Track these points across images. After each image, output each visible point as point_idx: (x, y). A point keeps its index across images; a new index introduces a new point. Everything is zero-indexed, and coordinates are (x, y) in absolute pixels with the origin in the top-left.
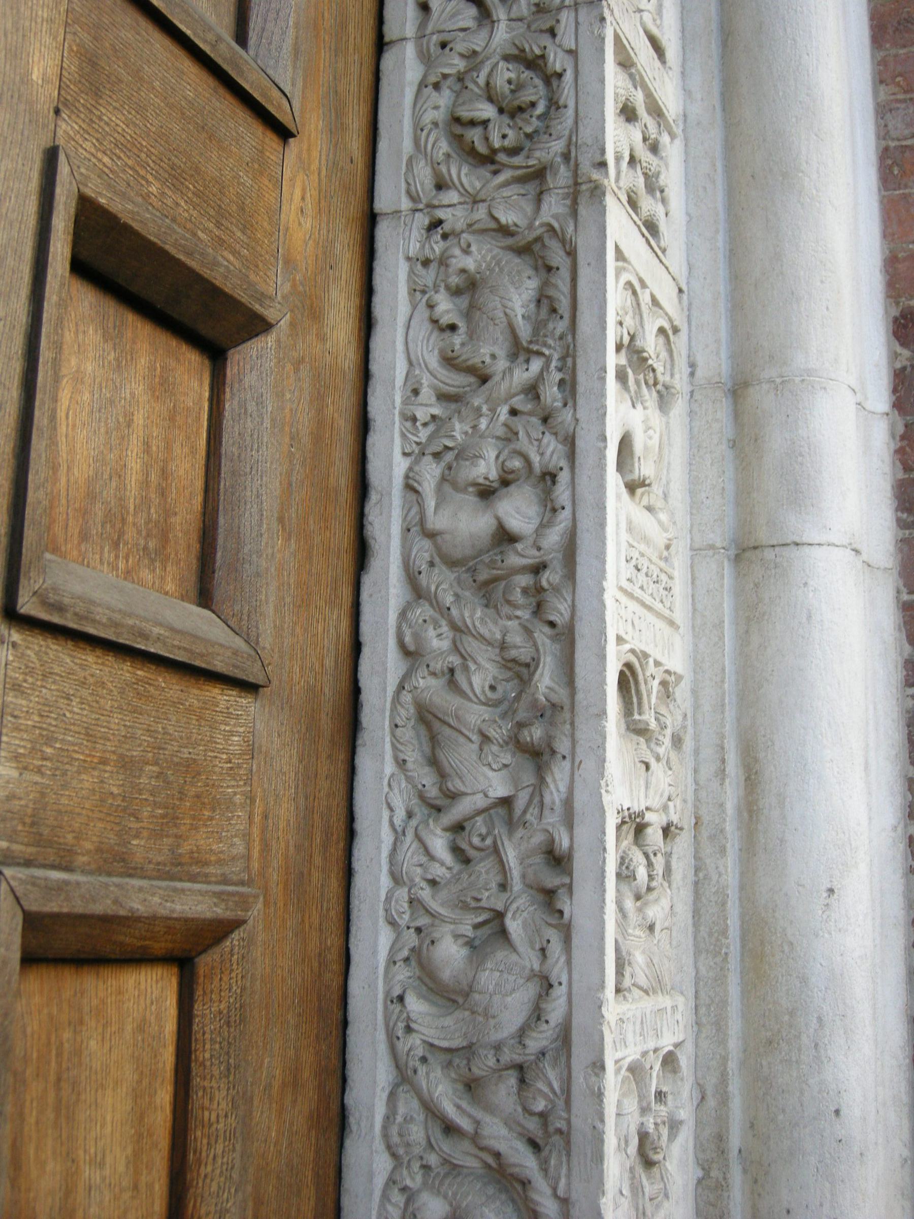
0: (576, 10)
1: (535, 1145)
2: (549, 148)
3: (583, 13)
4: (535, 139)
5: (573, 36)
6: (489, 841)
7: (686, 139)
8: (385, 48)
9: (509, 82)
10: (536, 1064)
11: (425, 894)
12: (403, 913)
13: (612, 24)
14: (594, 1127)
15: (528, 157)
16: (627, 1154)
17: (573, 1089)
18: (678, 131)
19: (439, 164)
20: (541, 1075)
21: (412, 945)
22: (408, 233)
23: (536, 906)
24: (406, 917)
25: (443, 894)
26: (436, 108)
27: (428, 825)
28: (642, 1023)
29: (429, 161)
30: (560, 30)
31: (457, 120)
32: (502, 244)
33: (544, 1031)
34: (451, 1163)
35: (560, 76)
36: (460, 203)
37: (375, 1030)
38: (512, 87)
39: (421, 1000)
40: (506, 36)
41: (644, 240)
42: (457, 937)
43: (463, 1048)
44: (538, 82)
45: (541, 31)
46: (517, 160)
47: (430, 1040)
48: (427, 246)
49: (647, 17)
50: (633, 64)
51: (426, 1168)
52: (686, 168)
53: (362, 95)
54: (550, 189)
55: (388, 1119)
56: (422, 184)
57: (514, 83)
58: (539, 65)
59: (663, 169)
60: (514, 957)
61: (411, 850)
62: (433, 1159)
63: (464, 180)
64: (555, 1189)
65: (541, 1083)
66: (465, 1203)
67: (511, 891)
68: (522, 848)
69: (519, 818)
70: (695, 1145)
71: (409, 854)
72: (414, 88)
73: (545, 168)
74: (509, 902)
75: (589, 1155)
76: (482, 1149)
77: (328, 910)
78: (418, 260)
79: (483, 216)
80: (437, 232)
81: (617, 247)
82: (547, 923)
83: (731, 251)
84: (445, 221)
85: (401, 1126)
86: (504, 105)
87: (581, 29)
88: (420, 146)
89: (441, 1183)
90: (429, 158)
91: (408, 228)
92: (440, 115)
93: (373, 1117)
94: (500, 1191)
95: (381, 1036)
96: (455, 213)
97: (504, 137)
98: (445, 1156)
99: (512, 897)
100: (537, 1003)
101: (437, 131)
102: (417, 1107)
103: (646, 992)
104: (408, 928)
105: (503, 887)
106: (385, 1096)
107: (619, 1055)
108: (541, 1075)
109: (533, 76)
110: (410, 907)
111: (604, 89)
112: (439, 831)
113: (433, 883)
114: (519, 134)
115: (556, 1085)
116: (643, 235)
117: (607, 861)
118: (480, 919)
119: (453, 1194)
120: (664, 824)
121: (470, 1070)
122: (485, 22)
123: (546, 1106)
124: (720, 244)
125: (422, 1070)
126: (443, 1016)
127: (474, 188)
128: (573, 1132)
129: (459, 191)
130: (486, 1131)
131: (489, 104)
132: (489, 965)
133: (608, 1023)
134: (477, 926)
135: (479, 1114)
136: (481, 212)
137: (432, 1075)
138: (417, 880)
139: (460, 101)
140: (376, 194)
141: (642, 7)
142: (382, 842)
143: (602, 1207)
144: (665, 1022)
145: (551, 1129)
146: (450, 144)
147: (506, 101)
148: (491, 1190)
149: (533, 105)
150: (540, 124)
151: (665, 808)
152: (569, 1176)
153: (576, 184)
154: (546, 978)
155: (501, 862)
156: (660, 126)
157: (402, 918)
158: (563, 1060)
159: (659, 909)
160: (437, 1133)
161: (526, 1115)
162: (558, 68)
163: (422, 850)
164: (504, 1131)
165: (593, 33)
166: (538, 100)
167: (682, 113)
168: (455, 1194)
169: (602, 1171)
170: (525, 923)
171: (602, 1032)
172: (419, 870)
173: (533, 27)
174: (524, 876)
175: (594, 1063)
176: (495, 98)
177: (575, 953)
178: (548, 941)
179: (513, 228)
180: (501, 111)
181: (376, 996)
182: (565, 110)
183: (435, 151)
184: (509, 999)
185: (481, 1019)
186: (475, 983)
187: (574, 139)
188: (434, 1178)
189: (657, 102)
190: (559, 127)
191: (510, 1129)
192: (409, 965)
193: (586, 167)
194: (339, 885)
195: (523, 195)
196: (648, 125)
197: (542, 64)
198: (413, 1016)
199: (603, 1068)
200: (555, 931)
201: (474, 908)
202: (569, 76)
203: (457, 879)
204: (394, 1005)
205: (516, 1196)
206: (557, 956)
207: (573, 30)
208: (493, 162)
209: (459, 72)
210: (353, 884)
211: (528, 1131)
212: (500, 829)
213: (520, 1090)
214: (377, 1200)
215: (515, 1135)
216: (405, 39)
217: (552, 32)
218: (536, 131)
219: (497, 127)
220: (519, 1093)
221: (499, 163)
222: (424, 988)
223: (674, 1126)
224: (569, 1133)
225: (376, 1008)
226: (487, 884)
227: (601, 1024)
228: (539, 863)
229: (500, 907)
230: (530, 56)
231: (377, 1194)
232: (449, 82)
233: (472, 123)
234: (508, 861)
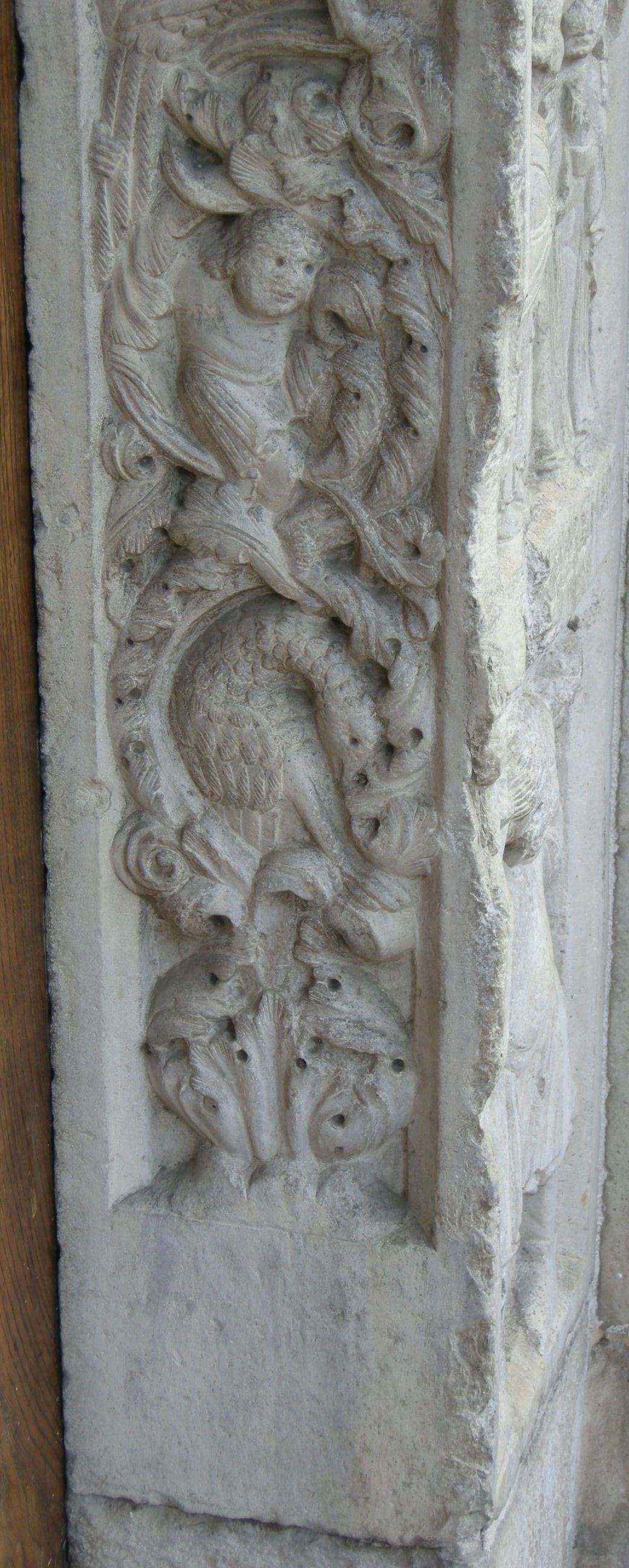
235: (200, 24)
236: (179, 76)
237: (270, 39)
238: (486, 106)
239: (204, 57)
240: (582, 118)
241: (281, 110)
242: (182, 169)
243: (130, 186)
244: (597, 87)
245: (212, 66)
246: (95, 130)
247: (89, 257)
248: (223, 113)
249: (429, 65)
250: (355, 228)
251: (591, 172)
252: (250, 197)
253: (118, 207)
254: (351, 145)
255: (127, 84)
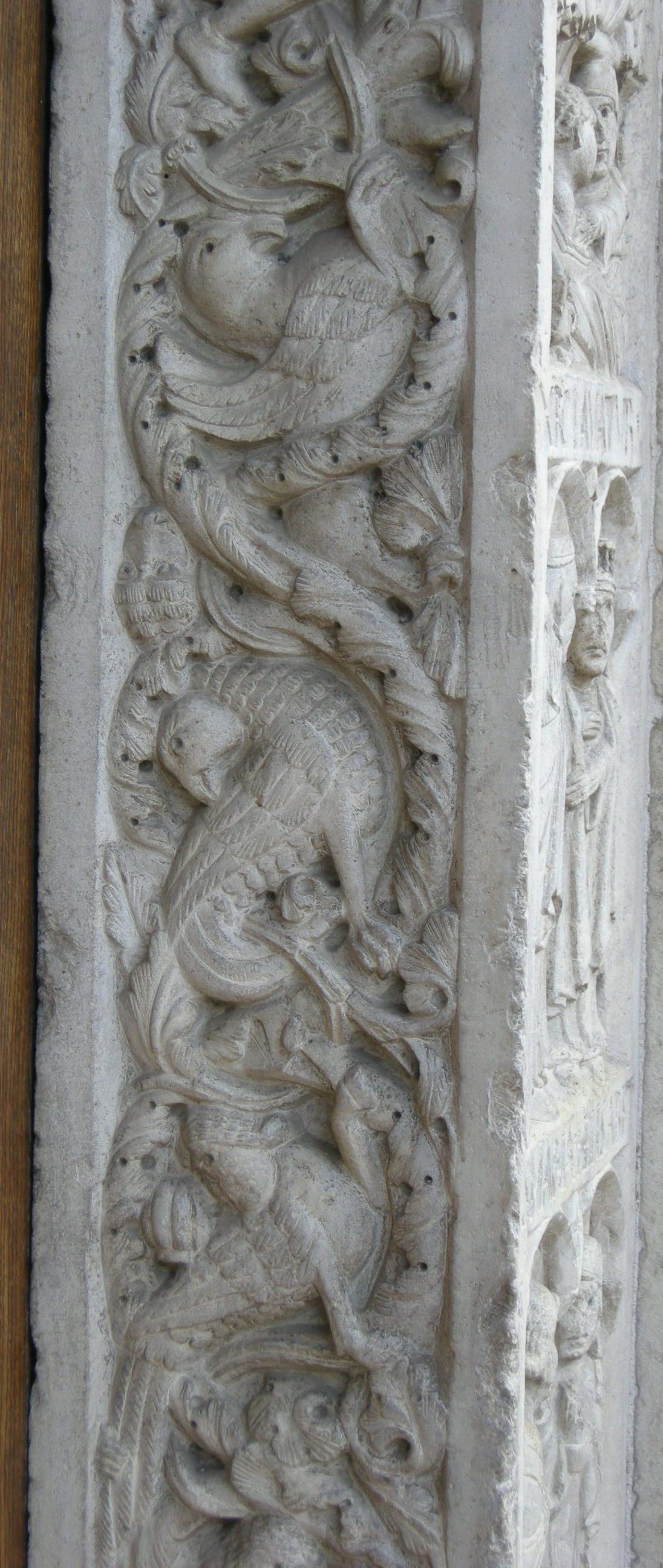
1: (401, 609)
6: (317, 59)
10: (407, 462)
11: (194, 159)
12: (153, 195)
14: (514, 570)
16: (558, 636)
17: (476, 504)
20: (416, 482)
21: (171, 254)
23: (406, 178)
24: (158, 203)
25: (230, 159)
27: (201, 29)
28: (584, 410)
33: (421, 403)
34: (244, 646)
37: (102, 411)
39: (189, 357)
42: (256, 236)
43: (268, 440)
47: (206, 428)
51: (198, 658)
55: (127, 574)
60: (366, 270)
61: (166, 77)
62: (211, 642)
64: (440, 684)
65: (417, 496)
66: (272, 717)
67: (359, 150)
68: (381, 68)
69: (376, 14)
70: (651, 661)
71: (163, 84)
74: (357, 168)
75: (504, 619)
76: (302, 619)
77: (14, 185)
82: (428, 206)
85: (152, 583)
89: (227, 685)
93: (99, 569)
94: (336, 693)
95: (113, 423)
98: (233, 634)
99: (362, 161)
100: (409, 354)
102: (182, 550)
103: (589, 355)
104: (162, 223)
105: (344, 144)
106: (120, 531)
107: (555, 452)
108: (416, 482)
110: (165, 185)
112: (221, 41)
113: (209, 139)
115: (443, 499)
117: (544, 89)
118: (300, 204)
119: (249, 702)
120: (618, 60)
121: (282, 477)
123: (423, 538)
125: (191, 481)
126: (228, 384)
128: (474, 582)
130: (311, 586)
132: (319, 286)
133: (541, 386)
134: (293, 218)
135: (298, 557)
137: (210, 490)
138: (179, 132)
142: (111, 63)
143: (527, 710)
144: (614, 422)
145: (434, 577)
148: (320, 693)
151: (618, 34)
152: (466, 659)
154: (427, 307)
155: (341, 96)
157: (150, 205)
158: (457, 452)
159: (610, 214)
160: (218, 597)
161: (387, 556)
163: (188, 77)
164: (345, 585)
168: (253, 702)
169: (529, 646)
170: (386, 209)
171: (530, 400)
172: (183, 115)
174: (383, 123)
175: (516, 457)
177: (484, 259)
178: (431, 240)
181: (102, 348)
184: (357, 346)
185: (302, 385)
186: (291, 321)
188: (213, 676)
191: (357, 581)
192: (164, 292)
194: (32, 143)
198: (173, 383)
199: (531, 465)
200: (445, 221)
201: (287, 184)
203: (254, 129)
204: (137, 366)
205: (365, 704)
206: (447, 265)
210: (54, 145)
211: (391, 583)
212: (338, 36)
213: (375, 510)
214: (109, 718)
215: (365, 591)
220: (373, 517)
222: (192, 336)
223: (624, 618)
224: (467, 585)
225: (103, 371)
226: (312, 137)
227: (530, 386)
228: (413, 98)
229: (338, 179)
231: (109, 707)
234: (355, 94)
235: (207, 1336)
236: (185, 1385)
237: (274, 1353)
238: (480, 1425)
239: (209, 1366)
240: (576, 1417)
241: (282, 1421)
242: (185, 1473)
243: (133, 1488)
244: (592, 1386)
245: (217, 1375)
246: (102, 1433)
247: (91, 1555)
248: (227, 1421)
249: (426, 1383)
250: (352, 1537)
251: (586, 1469)
252: (250, 1504)
253: (122, 1508)
254: (349, 1456)
255: (135, 1390)
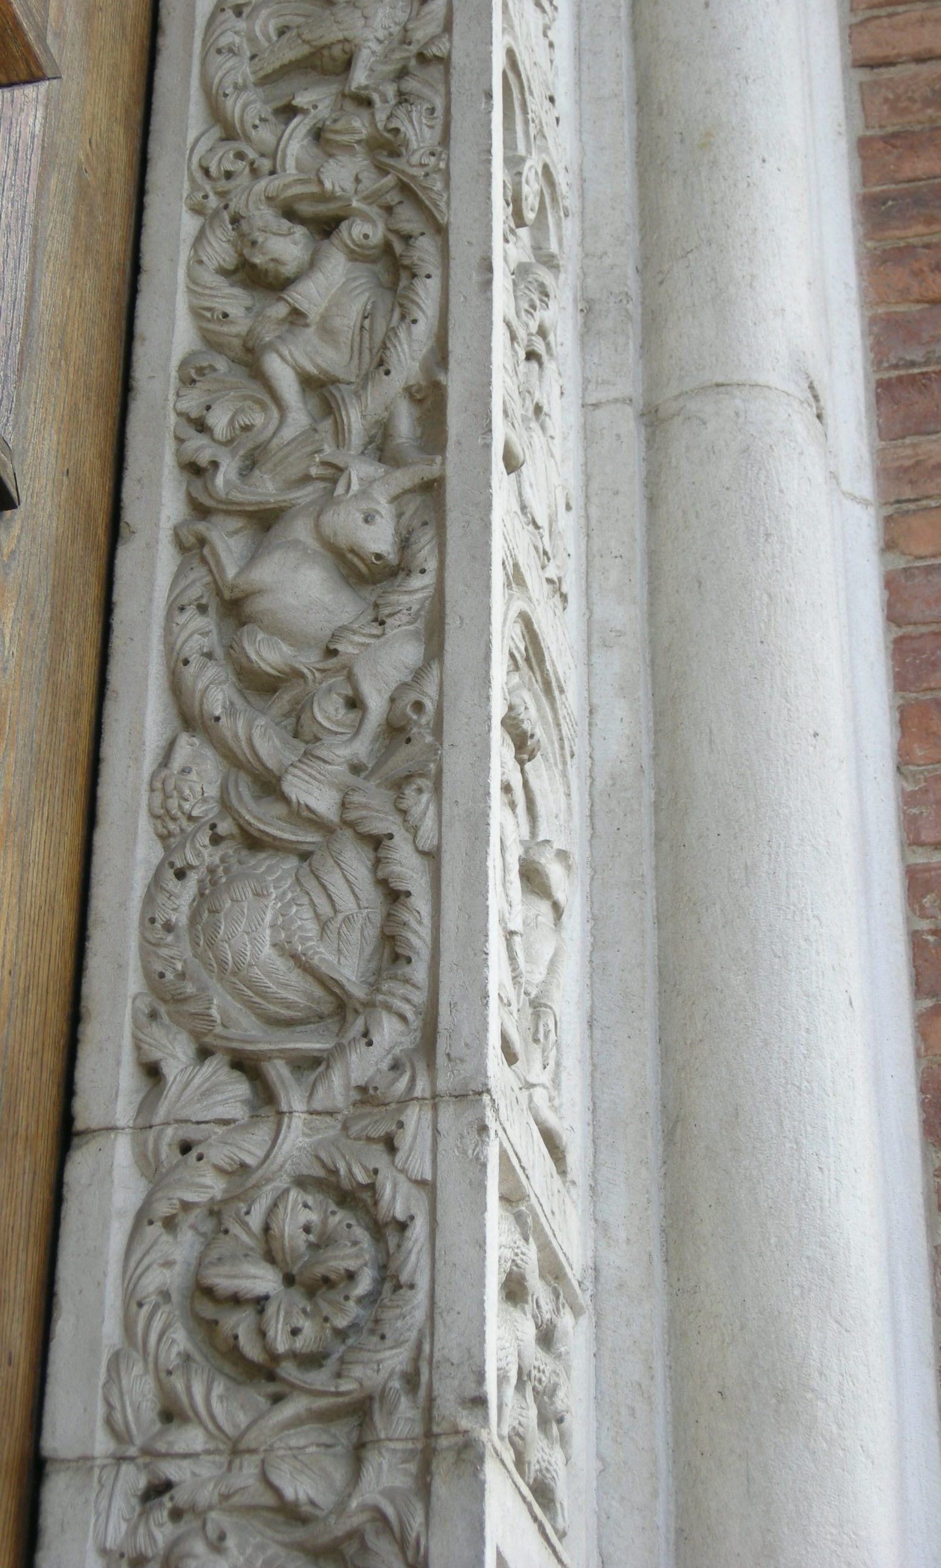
0: (435, 1108)
2: (379, 1362)
3: (447, 1114)
4: (351, 1341)
5: (428, 1157)
7: (598, 1314)
8: (76, 1141)
9: (307, 1229)
13: (496, 1134)
15: (339, 1375)
18: (584, 1299)
19: (169, 1373)
22: (104, 1503)
26: (168, 1264)
29: (151, 1366)
30: (404, 1142)
31: (208, 1292)
32: (286, 1538)
35: (402, 1227)
36: (208, 1452)
38: (312, 1238)
40: (303, 1141)
41: (535, 1527)
44: (360, 1233)
45: (369, 1139)
46: (318, 1378)
48: (141, 1530)
49: (540, 1096)
50: (524, 1197)
52: (597, 1368)
53: (32, 1229)
54: (379, 1440)
56: (137, 1410)
57: (317, 1230)
58: (365, 1201)
59: (563, 1376)
63: (217, 1407)
72: (128, 1223)
73: (370, 1398)
78: (122, 1555)
79: (251, 1482)
80: (161, 1505)
81: (499, 1553)
83: (679, 1531)
84: (179, 1484)
86: (295, 1271)
87: (443, 1144)
88: (135, 1334)
90: (151, 1359)
91: (106, 1492)
92: (174, 1279)
96: (197, 1470)
97: (295, 1332)
101: (166, 1308)
109: (353, 1222)
111: (484, 1259)
114: (323, 1328)
116: (535, 1519)
122: (264, 1111)
124: (660, 1519)
127: (236, 1426)
129: (206, 1429)
131: (268, 1266)
136: (247, 1474)
139: (214, 1255)
140: (47, 1420)
141: (533, 1079)
146: (190, 1333)
147: (300, 1264)
149: (351, 1276)
150: (362, 1312)
153: (429, 1434)
156: (558, 1297)
162: (400, 1214)
165: (465, 1152)
166: (361, 1268)
167: (591, 1265)
173: (355, 1129)
176: (279, 1257)
179: (306, 1509)
180: (289, 1280)
182: (410, 1293)
183: (163, 1347)
187: (427, 1348)
189: (556, 1256)
190: (399, 1324)
193: (447, 1404)
195: (328, 1446)
196: (542, 1303)
197: (369, 1201)
202: (419, 1230)
207: (429, 1143)
208: (271, 1377)
209: (212, 1199)
216: (113, 1128)
217: (390, 1145)
218: (354, 1326)
219: (282, 1313)
221: (284, 1381)
230: (346, 1184)
232: (193, 1216)
233: (236, 1300)
